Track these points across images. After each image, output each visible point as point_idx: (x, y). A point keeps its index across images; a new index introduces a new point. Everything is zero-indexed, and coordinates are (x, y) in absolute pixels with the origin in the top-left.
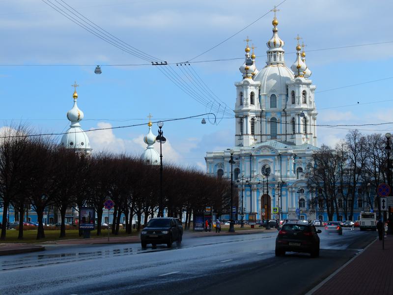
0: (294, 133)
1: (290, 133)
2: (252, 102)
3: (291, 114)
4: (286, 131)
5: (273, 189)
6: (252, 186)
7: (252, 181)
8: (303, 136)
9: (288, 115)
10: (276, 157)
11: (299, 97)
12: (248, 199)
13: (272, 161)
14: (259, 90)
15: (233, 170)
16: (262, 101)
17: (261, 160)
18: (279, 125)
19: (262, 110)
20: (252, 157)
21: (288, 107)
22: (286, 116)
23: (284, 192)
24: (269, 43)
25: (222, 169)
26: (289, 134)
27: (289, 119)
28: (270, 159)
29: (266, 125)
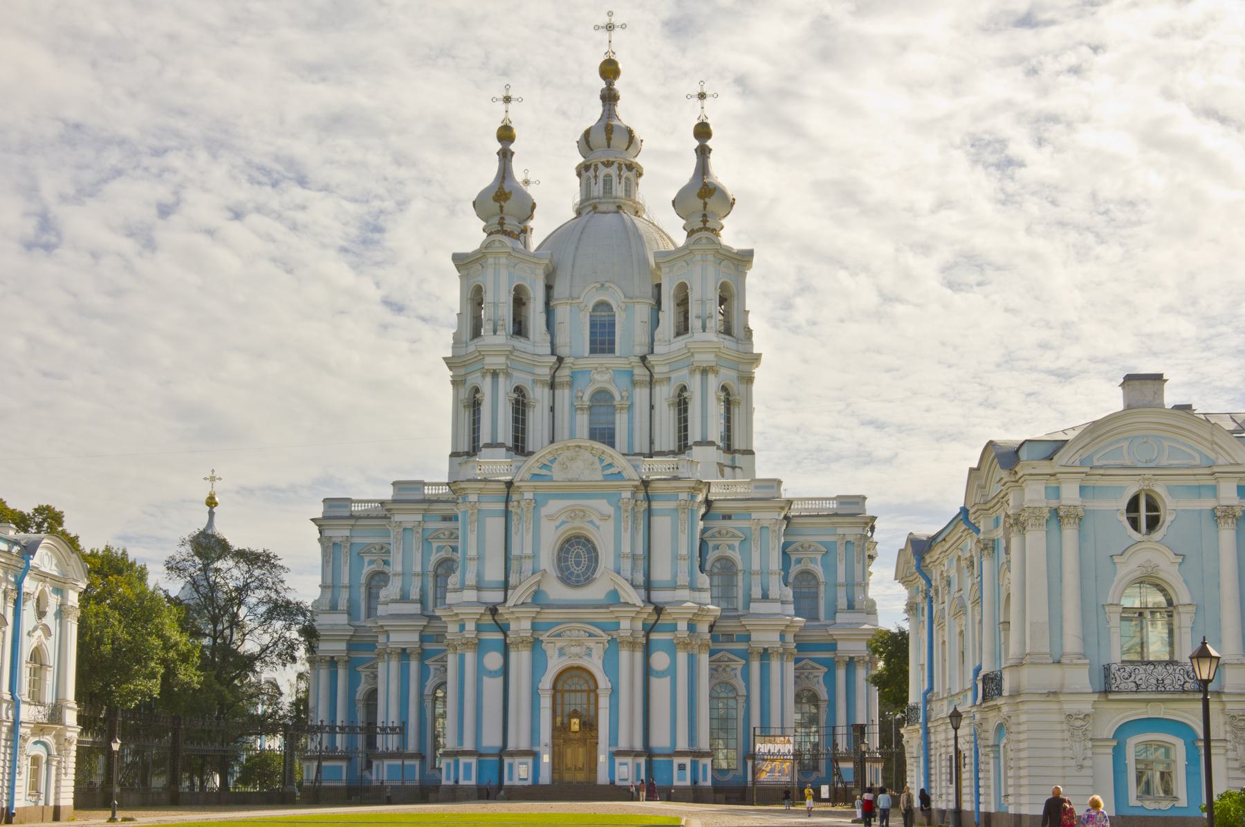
0: (683, 446)
1: (665, 449)
2: (520, 329)
3: (674, 375)
4: (651, 442)
5: (613, 641)
6: (513, 626)
7: (510, 603)
9: (661, 381)
10: (627, 494)
12: (493, 687)
14: (549, 288)
15: (431, 568)
16: (557, 327)
17: (554, 506)
20: (515, 497)
21: (656, 349)
22: (651, 383)
23: (660, 660)
25: (386, 569)
27: (664, 394)
28: (603, 506)
29: (572, 419)
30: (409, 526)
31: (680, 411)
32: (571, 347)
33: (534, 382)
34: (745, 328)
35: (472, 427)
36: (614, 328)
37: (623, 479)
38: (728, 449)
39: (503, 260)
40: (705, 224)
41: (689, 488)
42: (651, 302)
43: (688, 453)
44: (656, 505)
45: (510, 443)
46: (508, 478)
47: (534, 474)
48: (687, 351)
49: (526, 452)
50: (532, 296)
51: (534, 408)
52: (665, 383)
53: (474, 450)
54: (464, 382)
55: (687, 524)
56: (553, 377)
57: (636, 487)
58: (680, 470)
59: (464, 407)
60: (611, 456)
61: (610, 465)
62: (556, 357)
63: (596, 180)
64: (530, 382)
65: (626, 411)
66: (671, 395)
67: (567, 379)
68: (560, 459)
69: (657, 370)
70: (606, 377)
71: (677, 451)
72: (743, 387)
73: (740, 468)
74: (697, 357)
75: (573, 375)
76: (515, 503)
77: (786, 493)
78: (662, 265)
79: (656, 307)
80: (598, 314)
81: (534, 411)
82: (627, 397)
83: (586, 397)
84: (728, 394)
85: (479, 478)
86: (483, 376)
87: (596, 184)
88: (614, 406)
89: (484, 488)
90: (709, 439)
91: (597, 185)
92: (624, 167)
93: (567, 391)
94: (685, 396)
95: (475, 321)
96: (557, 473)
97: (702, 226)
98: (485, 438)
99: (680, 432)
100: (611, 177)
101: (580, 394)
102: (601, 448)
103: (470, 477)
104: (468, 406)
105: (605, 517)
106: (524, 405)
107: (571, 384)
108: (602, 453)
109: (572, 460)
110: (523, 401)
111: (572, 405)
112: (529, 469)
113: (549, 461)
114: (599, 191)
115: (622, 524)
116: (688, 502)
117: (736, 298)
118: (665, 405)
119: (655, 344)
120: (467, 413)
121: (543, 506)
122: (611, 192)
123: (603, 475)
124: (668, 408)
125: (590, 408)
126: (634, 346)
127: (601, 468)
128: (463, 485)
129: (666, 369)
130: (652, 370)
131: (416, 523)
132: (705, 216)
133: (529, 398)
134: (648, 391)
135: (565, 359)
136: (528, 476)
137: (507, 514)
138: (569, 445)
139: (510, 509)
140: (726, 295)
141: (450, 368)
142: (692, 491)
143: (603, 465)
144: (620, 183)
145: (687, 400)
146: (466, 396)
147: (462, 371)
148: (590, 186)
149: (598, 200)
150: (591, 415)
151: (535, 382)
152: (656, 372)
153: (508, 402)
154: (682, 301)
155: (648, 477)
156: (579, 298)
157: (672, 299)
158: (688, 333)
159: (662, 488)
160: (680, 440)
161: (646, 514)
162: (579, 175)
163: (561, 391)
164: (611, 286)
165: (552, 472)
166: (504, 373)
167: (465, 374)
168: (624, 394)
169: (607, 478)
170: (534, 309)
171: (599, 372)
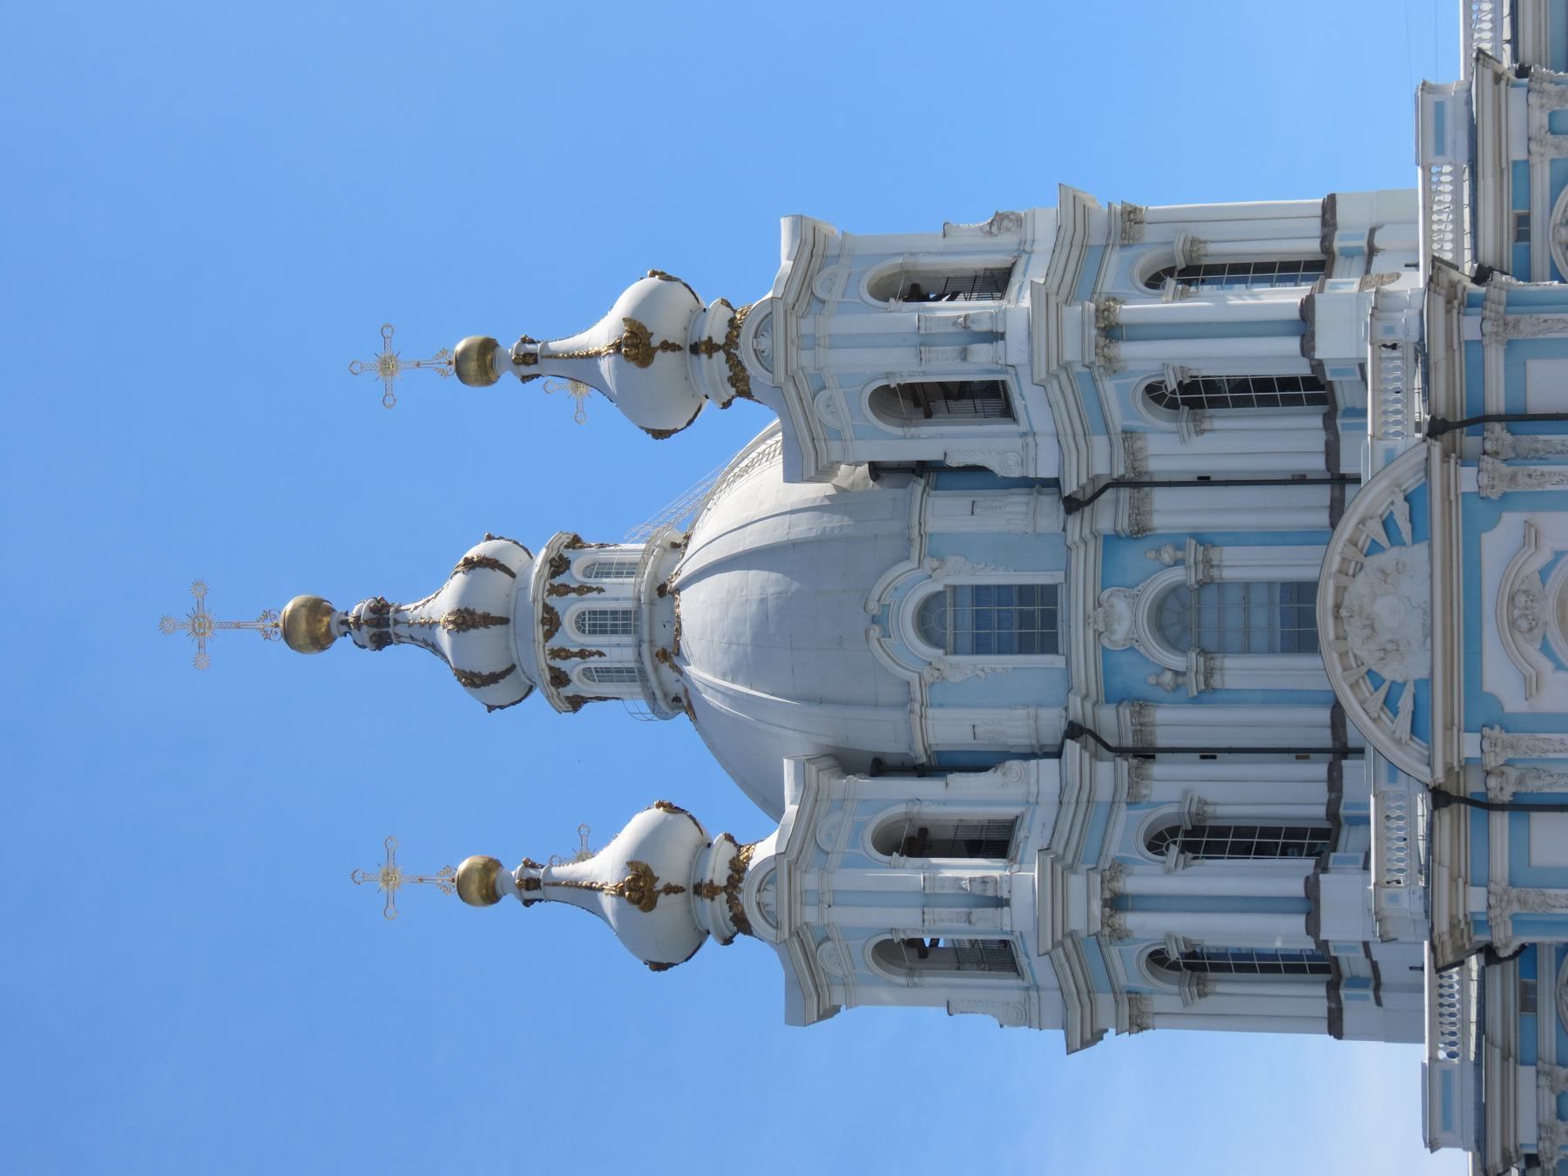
1: (1318, 441)
4: (1300, 480)
8: (1345, 284)
9: (1132, 455)
10: (1468, 479)
11: (924, 341)
13: (1511, 521)
14: (880, 767)
16: (983, 744)
17: (1499, 678)
18: (1238, 565)
19: (1075, 731)
20: (1473, 786)
21: (1047, 471)
22: (1137, 483)
24: (472, 680)
26: (1332, 451)
29: (1237, 698)
30: (1550, 1101)
31: (1214, 403)
32: (1040, 705)
33: (1137, 803)
34: (990, 233)
35: (1259, 976)
36: (987, 588)
37: (1425, 488)
38: (1318, 267)
39: (810, 881)
40: (717, 348)
41: (1448, 311)
42: (919, 489)
43: (1334, 372)
44: (1496, 401)
45: (1311, 862)
46: (1422, 807)
47: (1414, 731)
48: (1055, 383)
49: (1326, 825)
50: (901, 809)
51: (1206, 803)
52: (1139, 444)
53: (1324, 969)
54: (1134, 996)
55: (1547, 316)
56: (1120, 751)
57: (1446, 456)
58: (1397, 337)
59: (1202, 995)
60: (1362, 522)
61: (1388, 524)
62: (1069, 742)
63: (592, 654)
64: (1136, 813)
65: (1215, 554)
66: (1172, 426)
67: (1126, 712)
68: (1371, 662)
69: (1101, 468)
70: (1121, 607)
71: (1324, 409)
72: (1150, 234)
73: (1372, 232)
74: (1071, 353)
75: (1114, 697)
76: (1493, 782)
77: (1455, 73)
78: (824, 462)
79: (933, 476)
80: (949, 631)
81: (1217, 804)
82: (1178, 548)
83: (1177, 661)
84: (1169, 272)
85: (1422, 884)
86: (1119, 935)
87: (601, 654)
88: (1202, 585)
89: (1451, 869)
90: (1296, 315)
92: (558, 581)
93: (1161, 715)
94: (1175, 386)
95: (967, 965)
96: (1406, 669)
97: (720, 356)
98: (1286, 933)
99: (1272, 402)
100: (584, 613)
101: (1168, 677)
102: (1339, 549)
103: (1418, 906)
104: (1201, 983)
105: (1532, 535)
106: (1197, 830)
107: (1141, 704)
108: (1356, 545)
109: (1373, 629)
110: (1187, 833)
111: (1197, 701)
112: (1399, 742)
113: (1376, 689)
114: (618, 645)
115: (1549, 487)
116: (1487, 313)
117: (912, 260)
118: (1200, 444)
119: (1032, 475)
120: (1220, 988)
121: (1503, 708)
122: (625, 612)
123: (1414, 542)
124: (1206, 435)
125: (1203, 652)
126: (1039, 535)
127: (1396, 549)
128: (1443, 925)
129: (1100, 443)
130: (1108, 481)
131: (1543, 1081)
132: (695, 349)
133: (1180, 815)
134: (1159, 495)
135: (1071, 718)
136: (1417, 746)
137: (1521, 806)
138: (1332, 636)
139: (1506, 797)
140: (902, 286)
141: (1097, 1036)
142: (1456, 303)
143: (1382, 539)
145: (1187, 381)
146: (1175, 988)
147: (1105, 1001)
148: (608, 670)
149: (645, 648)
150: (1223, 650)
151: (1134, 802)
152: (1108, 472)
153: (1189, 870)
154: (917, 404)
155: (1418, 427)
156: (909, 683)
157: (913, 430)
158: (1003, 382)
159: (1450, 385)
160: (1296, 401)
161: (1517, 425)
162: (576, 703)
163: (1159, 731)
164: (876, 597)
165: (1404, 684)
166: (1112, 879)
167: (1114, 993)
168: (1167, 557)
169: (1420, 532)
170: (933, 802)
171: (1108, 626)
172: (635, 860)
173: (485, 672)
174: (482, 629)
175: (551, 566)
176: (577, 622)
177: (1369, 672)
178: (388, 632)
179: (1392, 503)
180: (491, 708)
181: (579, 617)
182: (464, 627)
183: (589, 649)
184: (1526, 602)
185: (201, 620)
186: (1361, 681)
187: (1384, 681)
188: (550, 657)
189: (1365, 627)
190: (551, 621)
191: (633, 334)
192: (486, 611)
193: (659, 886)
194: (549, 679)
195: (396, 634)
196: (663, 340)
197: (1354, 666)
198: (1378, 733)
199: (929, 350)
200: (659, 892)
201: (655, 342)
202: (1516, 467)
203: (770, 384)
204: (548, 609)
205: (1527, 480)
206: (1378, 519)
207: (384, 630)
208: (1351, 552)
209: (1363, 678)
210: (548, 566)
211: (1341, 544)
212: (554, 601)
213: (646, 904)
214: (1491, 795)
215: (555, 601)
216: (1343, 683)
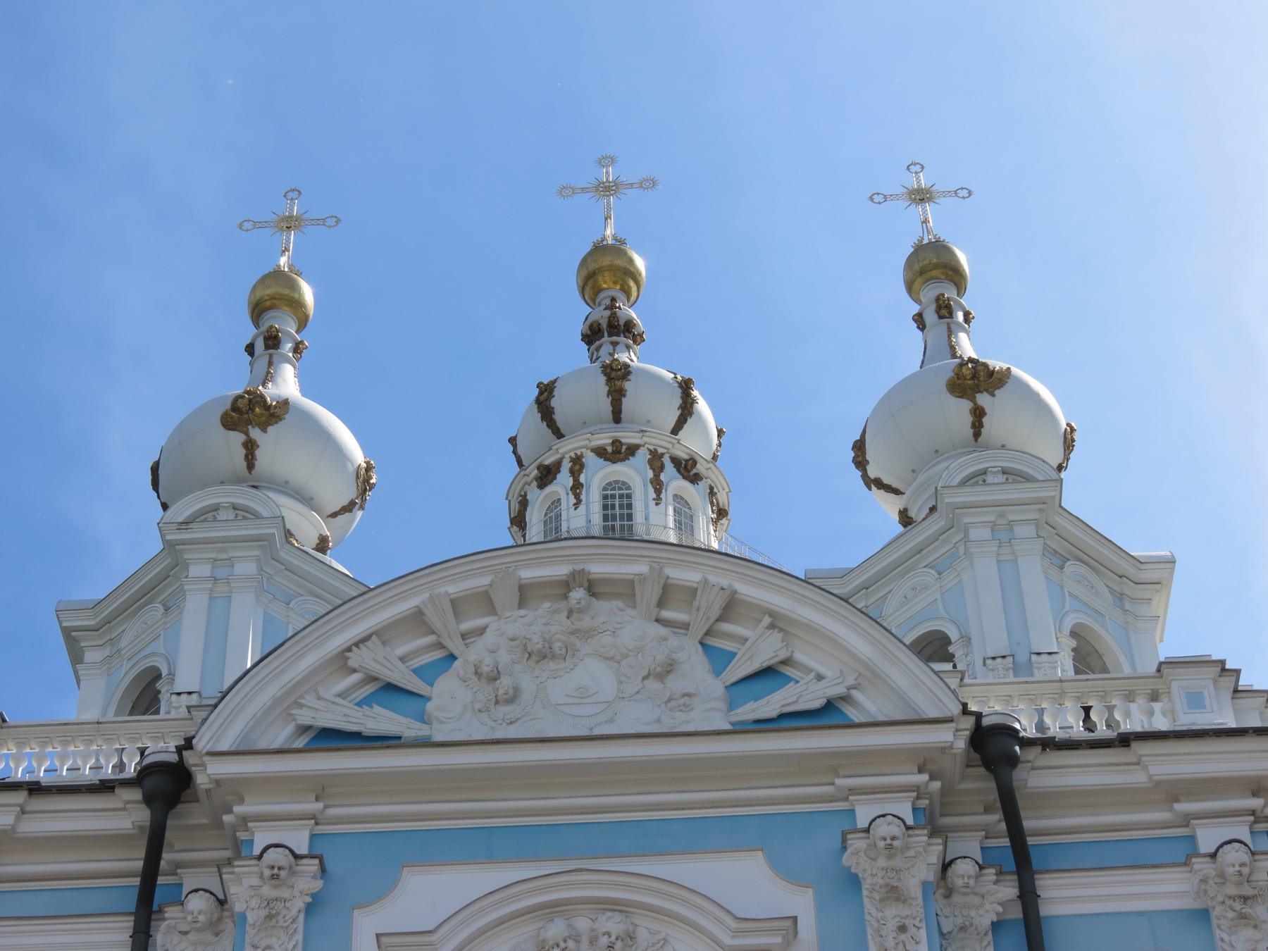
60: (778, 622)
63: (577, 497)
76: (198, 904)
87: (577, 505)
91: (582, 508)
100: (629, 488)
102: (713, 579)
113: (417, 671)
127: (716, 687)
138: (528, 574)
144: (658, 500)
172: (290, 407)
173: (554, 403)
174: (607, 388)
175: (687, 461)
176: (617, 482)
177: (452, 657)
178: (603, 336)
179: (820, 678)
180: (513, 441)
181: (624, 483)
182: (609, 370)
183: (584, 492)
184: (609, 934)
185: (614, 188)
186: (431, 639)
187: (431, 685)
188: (573, 456)
189: (549, 642)
190: (618, 453)
191: (991, 373)
192: (628, 394)
193: (255, 433)
194: (547, 462)
195: (600, 346)
196: (987, 411)
197: (467, 626)
198: (311, 660)
199: (1007, 670)
200: (247, 434)
201: (983, 399)
202: (920, 901)
203: (940, 485)
204: (632, 450)
205: (892, 924)
206: (783, 655)
207: (606, 334)
208: (712, 604)
209: (440, 646)
210: (686, 457)
211: (725, 582)
212: (642, 456)
213: (232, 418)
214: (171, 912)
215: (642, 456)
216: (426, 596)
